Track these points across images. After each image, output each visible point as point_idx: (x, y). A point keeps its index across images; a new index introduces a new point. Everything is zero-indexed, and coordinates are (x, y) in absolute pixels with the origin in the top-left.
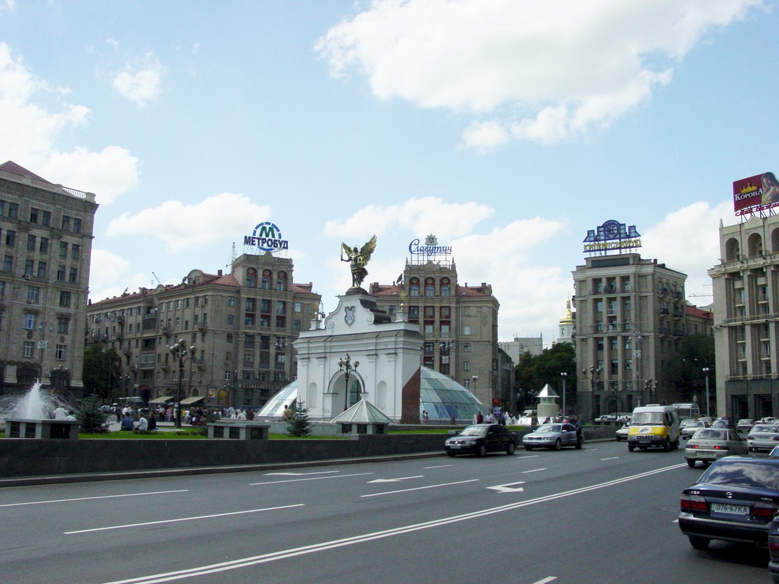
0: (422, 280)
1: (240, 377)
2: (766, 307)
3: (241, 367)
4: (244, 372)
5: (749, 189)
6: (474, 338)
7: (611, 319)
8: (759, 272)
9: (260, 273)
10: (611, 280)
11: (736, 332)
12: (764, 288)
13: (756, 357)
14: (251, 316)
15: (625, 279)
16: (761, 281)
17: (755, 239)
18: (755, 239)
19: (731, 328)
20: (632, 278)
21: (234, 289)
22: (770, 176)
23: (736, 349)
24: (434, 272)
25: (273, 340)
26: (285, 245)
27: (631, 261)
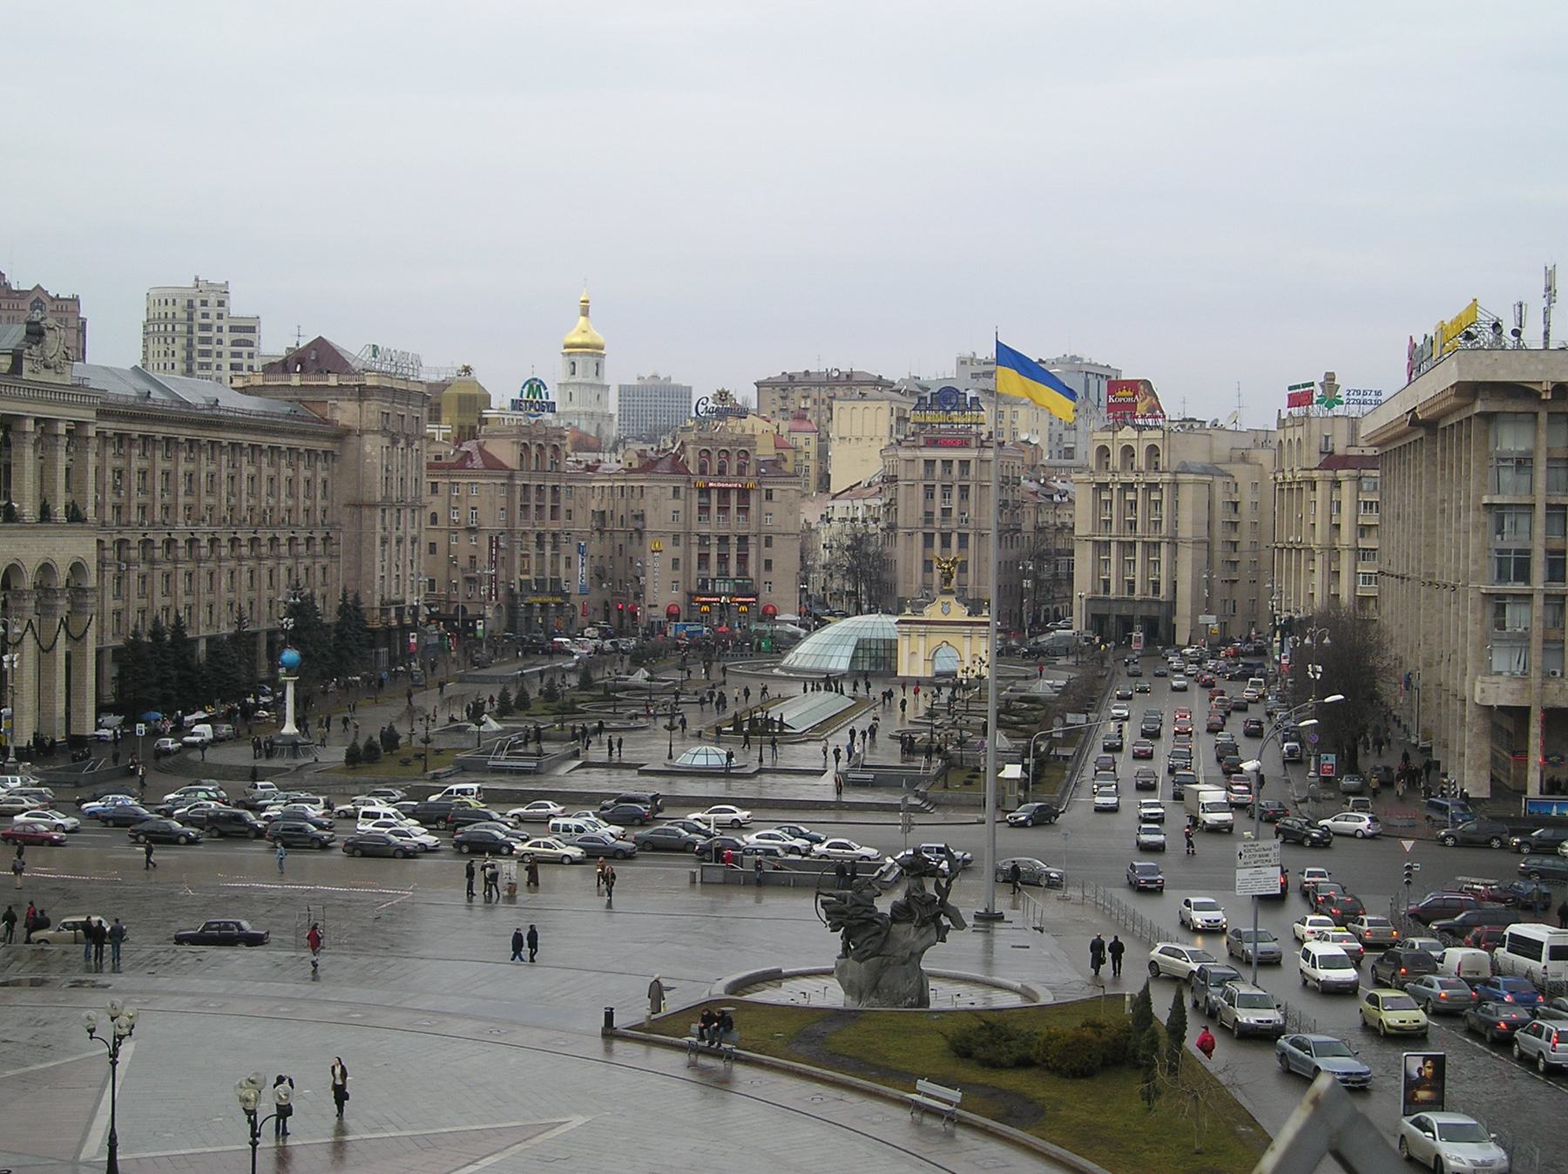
0: (715, 454)
1: (517, 590)
2: (1133, 524)
3: (518, 576)
4: (521, 581)
5: (1124, 393)
6: (777, 530)
7: (946, 512)
8: (1128, 486)
9: (534, 449)
10: (947, 463)
11: (1102, 547)
12: (1134, 504)
13: (1121, 574)
14: (524, 507)
15: (965, 464)
16: (1130, 496)
17: (1128, 451)
18: (1128, 451)
19: (1095, 542)
20: (972, 464)
21: (506, 473)
22: (1147, 383)
23: (1100, 563)
24: (729, 445)
25: (548, 538)
26: (551, 407)
27: (973, 443)
